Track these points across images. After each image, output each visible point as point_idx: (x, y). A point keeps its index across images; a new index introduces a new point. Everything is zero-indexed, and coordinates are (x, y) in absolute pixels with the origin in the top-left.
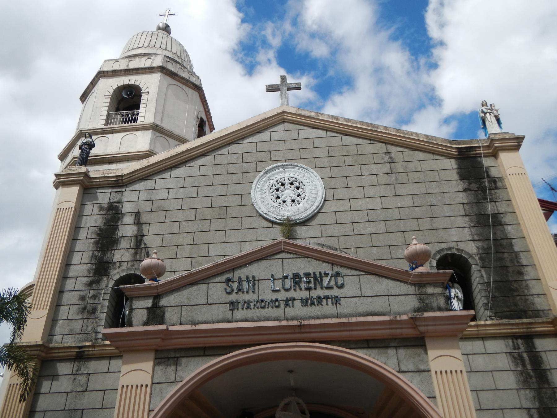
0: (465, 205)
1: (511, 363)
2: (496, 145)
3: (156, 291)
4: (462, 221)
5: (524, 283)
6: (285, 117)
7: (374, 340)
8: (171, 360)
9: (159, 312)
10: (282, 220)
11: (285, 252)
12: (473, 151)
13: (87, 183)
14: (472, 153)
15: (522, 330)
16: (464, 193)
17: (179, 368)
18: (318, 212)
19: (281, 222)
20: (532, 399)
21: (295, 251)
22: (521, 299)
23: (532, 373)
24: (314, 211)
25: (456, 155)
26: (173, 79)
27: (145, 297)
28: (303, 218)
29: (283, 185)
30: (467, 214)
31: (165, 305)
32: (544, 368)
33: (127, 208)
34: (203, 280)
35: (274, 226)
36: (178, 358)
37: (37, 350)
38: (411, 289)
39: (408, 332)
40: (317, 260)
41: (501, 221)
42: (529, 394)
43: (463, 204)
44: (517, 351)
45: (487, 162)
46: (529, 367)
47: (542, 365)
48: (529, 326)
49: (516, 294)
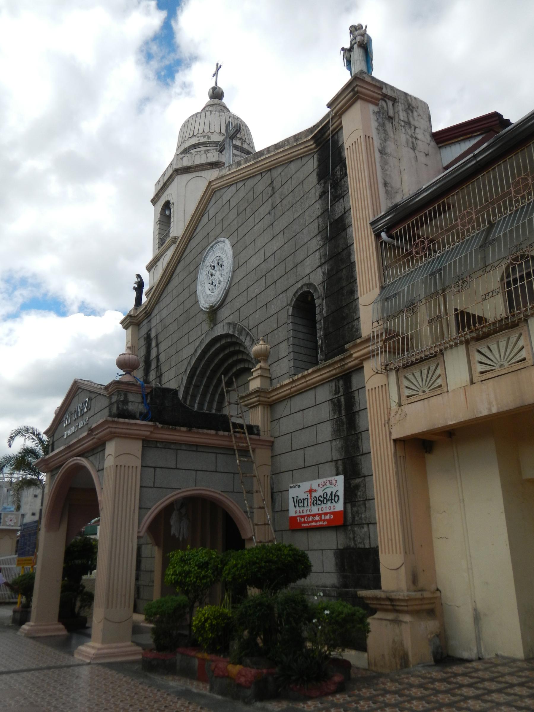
0: (319, 219)
1: (330, 411)
4: (316, 243)
5: (354, 304)
6: (213, 187)
12: (327, 131)
13: (137, 321)
14: (327, 134)
15: (337, 371)
16: (320, 201)
18: (229, 288)
20: (341, 449)
22: (349, 328)
23: (344, 420)
24: (225, 288)
25: (315, 148)
26: (190, 173)
28: (219, 300)
29: (214, 267)
30: (320, 230)
32: (354, 411)
33: (153, 334)
41: (345, 224)
42: (338, 444)
43: (318, 218)
44: (337, 396)
46: (343, 413)
47: (354, 408)
48: (343, 363)
49: (345, 323)
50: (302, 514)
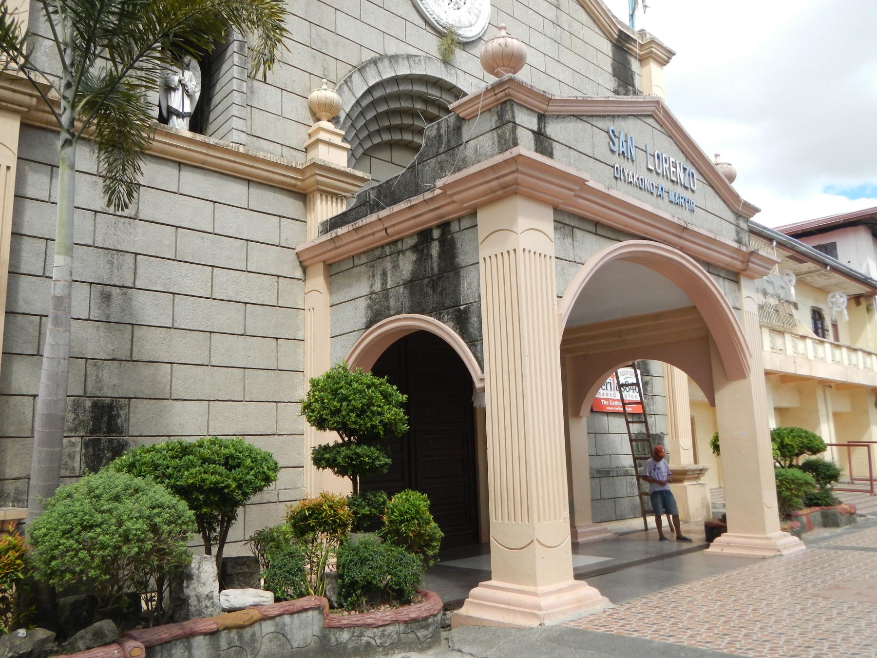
2: (653, 49)
3: (545, 107)
7: (712, 265)
8: (566, 227)
9: (547, 144)
10: (441, 26)
11: (654, 118)
17: (576, 244)
19: (441, 28)
21: (663, 123)
25: (614, 39)
27: (527, 108)
31: (552, 137)
34: (587, 116)
35: (428, 29)
36: (573, 227)
37: (31, 95)
38: (731, 217)
39: (738, 265)
40: (677, 145)
45: (635, 65)
50: (605, 397)
